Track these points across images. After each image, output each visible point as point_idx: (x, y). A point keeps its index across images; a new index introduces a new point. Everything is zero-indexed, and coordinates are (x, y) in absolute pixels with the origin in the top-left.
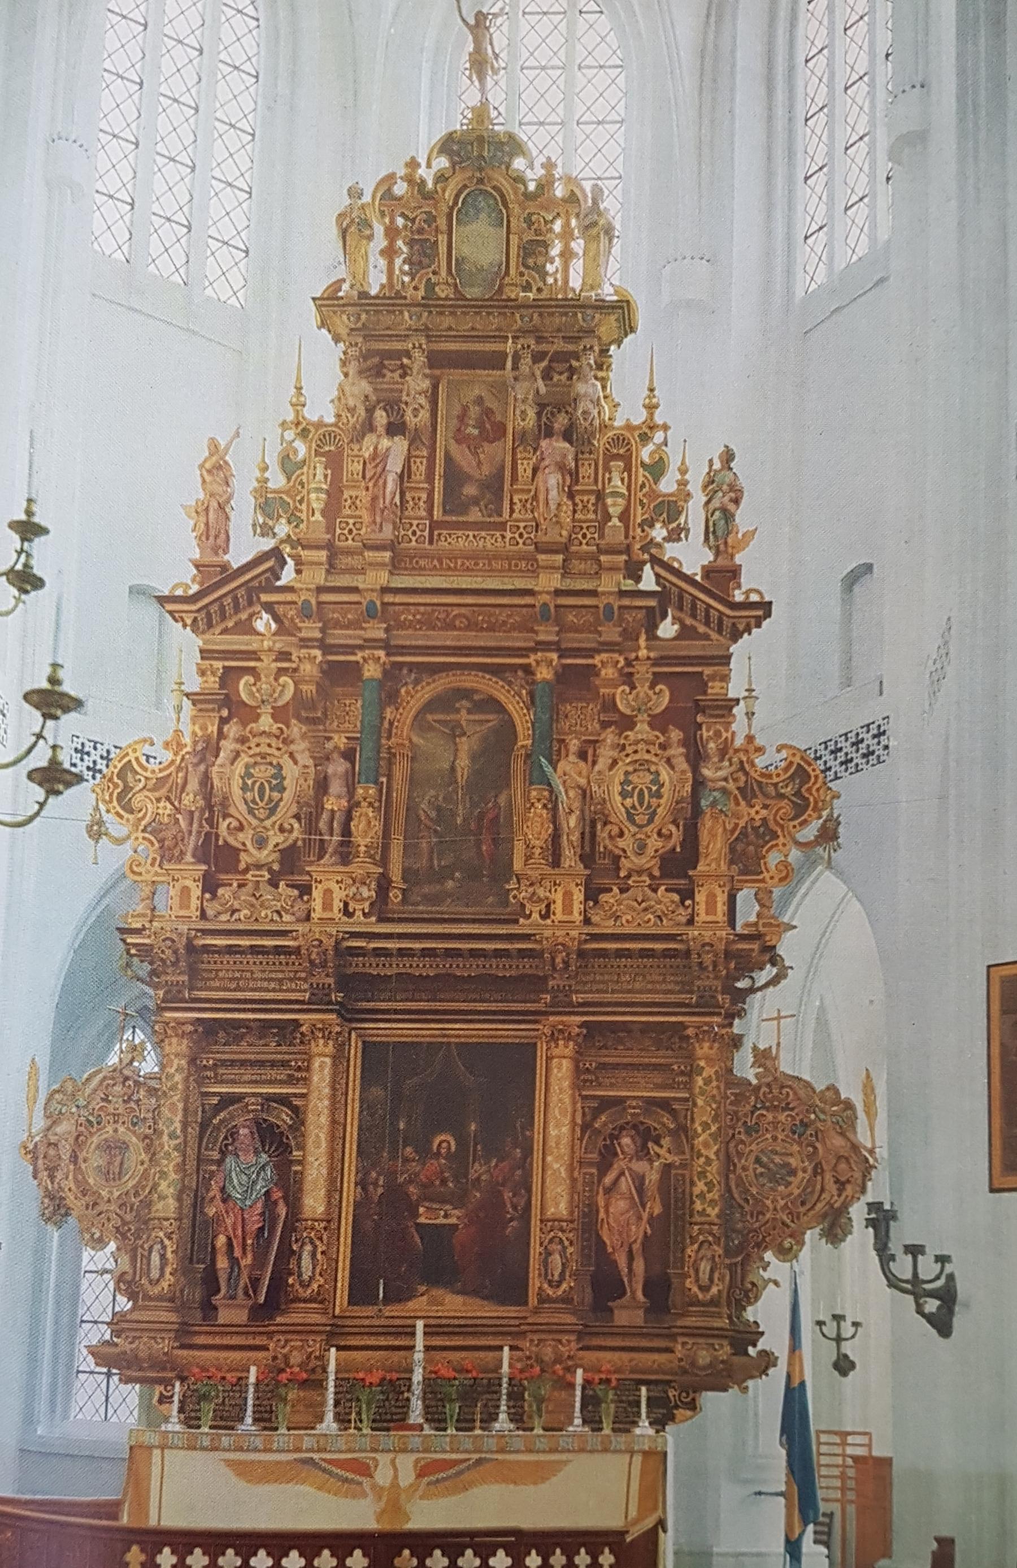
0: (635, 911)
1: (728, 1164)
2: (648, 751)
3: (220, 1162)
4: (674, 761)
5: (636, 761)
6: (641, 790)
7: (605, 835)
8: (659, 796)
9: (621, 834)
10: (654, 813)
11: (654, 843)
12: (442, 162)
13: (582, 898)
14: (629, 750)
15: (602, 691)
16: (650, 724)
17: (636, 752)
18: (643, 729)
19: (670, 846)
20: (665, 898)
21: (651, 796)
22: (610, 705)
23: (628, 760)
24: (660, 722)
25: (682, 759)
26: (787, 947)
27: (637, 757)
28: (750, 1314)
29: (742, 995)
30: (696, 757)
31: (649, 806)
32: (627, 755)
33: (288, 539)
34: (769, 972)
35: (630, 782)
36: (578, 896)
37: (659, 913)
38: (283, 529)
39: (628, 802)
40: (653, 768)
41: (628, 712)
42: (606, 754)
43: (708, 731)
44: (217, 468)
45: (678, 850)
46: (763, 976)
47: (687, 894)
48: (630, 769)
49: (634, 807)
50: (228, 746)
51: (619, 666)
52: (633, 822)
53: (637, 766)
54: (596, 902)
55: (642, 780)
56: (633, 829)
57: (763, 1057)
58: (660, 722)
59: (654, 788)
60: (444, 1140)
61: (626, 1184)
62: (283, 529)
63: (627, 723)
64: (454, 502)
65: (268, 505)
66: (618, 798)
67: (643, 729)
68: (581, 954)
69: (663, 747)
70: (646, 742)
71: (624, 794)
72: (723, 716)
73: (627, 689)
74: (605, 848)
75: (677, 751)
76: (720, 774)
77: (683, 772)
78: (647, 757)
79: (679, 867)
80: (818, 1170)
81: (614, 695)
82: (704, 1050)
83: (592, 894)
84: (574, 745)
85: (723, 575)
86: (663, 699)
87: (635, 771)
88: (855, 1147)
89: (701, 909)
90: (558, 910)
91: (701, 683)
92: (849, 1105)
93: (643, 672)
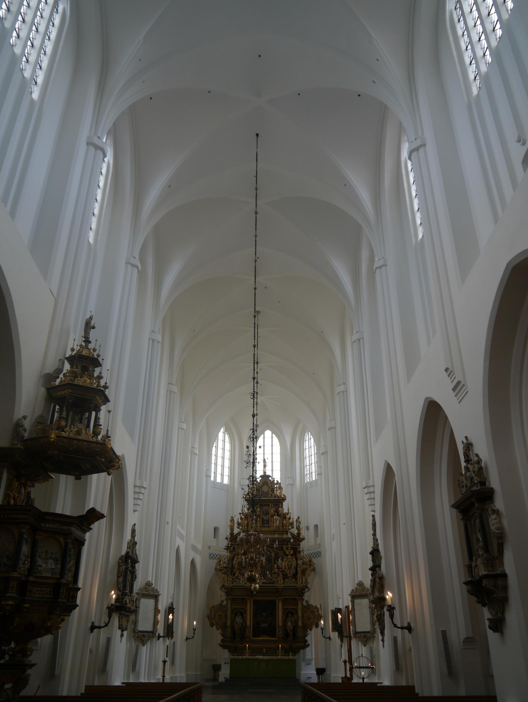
0: (290, 583)
1: (303, 617)
3: (235, 618)
11: (292, 572)
12: (260, 478)
20: (294, 580)
24: (292, 555)
26: (309, 586)
28: (306, 638)
29: (303, 593)
30: (297, 560)
33: (242, 529)
34: (307, 590)
36: (282, 580)
38: (241, 527)
42: (285, 560)
44: (232, 520)
46: (306, 590)
47: (296, 579)
50: (235, 559)
57: (307, 602)
58: (292, 555)
60: (264, 614)
61: (290, 621)
62: (241, 527)
64: (263, 524)
65: (239, 524)
68: (283, 589)
79: (295, 575)
80: (314, 617)
82: (299, 602)
83: (284, 579)
85: (299, 534)
86: (292, 552)
88: (319, 614)
90: (280, 583)
91: (296, 548)
92: (318, 608)
93: (289, 549)
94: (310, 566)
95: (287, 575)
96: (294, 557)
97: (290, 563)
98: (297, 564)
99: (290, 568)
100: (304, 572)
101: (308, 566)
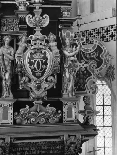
2: (41, 44)
4: (52, 48)
5: (36, 48)
6: (38, 61)
7: (22, 82)
8: (46, 64)
9: (30, 80)
10: (44, 71)
11: (45, 85)
13: (12, 111)
14: (32, 43)
15: (20, 16)
16: (41, 32)
17: (35, 44)
18: (38, 34)
19: (51, 85)
21: (43, 64)
22: (23, 22)
23: (32, 48)
24: (45, 31)
25: (56, 47)
27: (36, 47)
30: (61, 45)
31: (42, 69)
32: (32, 46)
35: (33, 58)
36: (11, 111)
37: (47, 117)
39: (33, 67)
40: (43, 51)
41: (31, 26)
42: (22, 45)
43: (64, 33)
45: (55, 87)
48: (33, 52)
49: (35, 69)
51: (27, 5)
52: (35, 76)
53: (36, 51)
54: (19, 112)
55: (38, 57)
56: (35, 79)
58: (45, 31)
59: (44, 61)
63: (31, 31)
66: (28, 65)
67: (38, 34)
69: (47, 42)
70: (40, 40)
71: (31, 63)
72: (69, 26)
73: (31, 16)
74: (22, 86)
75: (53, 44)
76: (72, 54)
77: (56, 53)
78: (41, 47)
79: (55, 97)
81: (25, 18)
84: (7, 40)
86: (47, 21)
87: (35, 52)
89: (66, 115)
94: (99, 64)
95: (27, 93)
96: (52, 37)
97: (38, 57)
98: (63, 57)
99: (39, 72)
100: (80, 84)
101: (95, 65)
